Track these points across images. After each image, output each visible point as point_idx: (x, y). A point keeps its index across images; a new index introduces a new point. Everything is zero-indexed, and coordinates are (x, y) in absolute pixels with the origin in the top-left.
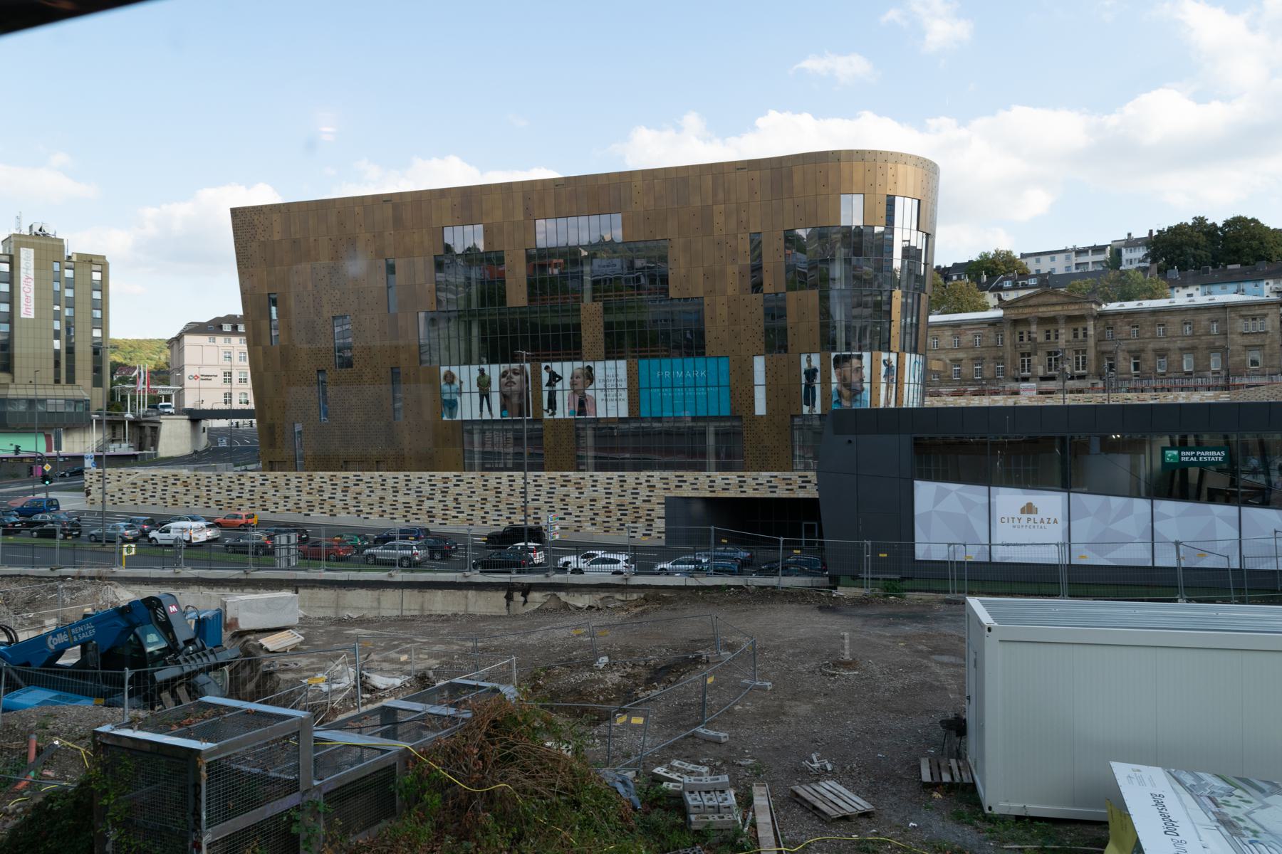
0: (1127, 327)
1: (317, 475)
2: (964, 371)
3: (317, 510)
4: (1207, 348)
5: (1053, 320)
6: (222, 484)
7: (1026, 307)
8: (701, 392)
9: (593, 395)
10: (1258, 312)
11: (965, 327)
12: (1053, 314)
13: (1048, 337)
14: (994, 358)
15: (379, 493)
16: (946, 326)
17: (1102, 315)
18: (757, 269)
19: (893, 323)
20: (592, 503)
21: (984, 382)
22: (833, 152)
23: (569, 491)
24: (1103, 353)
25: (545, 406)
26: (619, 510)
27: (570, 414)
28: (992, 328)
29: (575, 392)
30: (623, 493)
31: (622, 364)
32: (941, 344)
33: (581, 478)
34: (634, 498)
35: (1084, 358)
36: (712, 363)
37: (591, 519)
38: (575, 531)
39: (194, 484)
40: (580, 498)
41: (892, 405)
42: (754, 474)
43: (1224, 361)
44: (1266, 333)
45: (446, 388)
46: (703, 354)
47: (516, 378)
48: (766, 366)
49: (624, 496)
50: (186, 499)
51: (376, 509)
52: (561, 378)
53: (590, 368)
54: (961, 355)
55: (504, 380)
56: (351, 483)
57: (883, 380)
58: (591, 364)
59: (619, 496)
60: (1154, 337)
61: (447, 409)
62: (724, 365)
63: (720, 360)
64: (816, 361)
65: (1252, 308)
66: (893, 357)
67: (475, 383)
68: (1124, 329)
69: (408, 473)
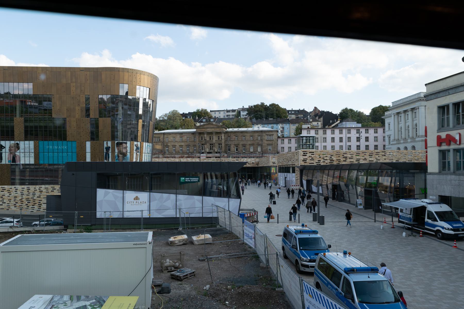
0: (234, 137)
2: (184, 149)
4: (257, 144)
5: (211, 133)
7: (203, 128)
8: (65, 154)
9: (19, 155)
10: (271, 134)
11: (183, 134)
12: (211, 131)
13: (210, 139)
14: (193, 145)
16: (177, 133)
17: (227, 132)
18: (88, 110)
19: (139, 131)
20: (15, 198)
21: (190, 154)
22: (117, 68)
23: (4, 193)
24: (227, 145)
26: (27, 201)
27: (8, 162)
28: (193, 135)
29: (11, 153)
30: (29, 194)
31: (32, 143)
32: (176, 140)
33: (10, 188)
34: (33, 196)
35: (221, 146)
36: (70, 144)
37: (14, 205)
38: (7, 210)
40: (9, 196)
41: (138, 161)
43: (262, 149)
44: (273, 140)
46: (65, 139)
48: (91, 145)
49: (29, 195)
52: (4, 147)
54: (183, 144)
57: (135, 152)
58: (18, 142)
59: (27, 195)
60: (242, 140)
62: (74, 144)
63: (73, 142)
64: (110, 144)
65: (269, 132)
66: (139, 143)
68: (233, 137)
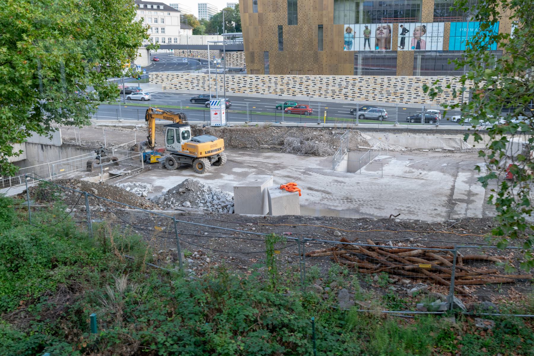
1: (286, 77)
6: (235, 80)
15: (319, 85)
25: (399, 44)
27: (412, 48)
29: (415, 38)
31: (442, 25)
39: (219, 80)
45: (346, 35)
47: (385, 31)
52: (408, 31)
53: (424, 27)
55: (378, 32)
56: (304, 80)
67: (362, 33)
69: (334, 76)
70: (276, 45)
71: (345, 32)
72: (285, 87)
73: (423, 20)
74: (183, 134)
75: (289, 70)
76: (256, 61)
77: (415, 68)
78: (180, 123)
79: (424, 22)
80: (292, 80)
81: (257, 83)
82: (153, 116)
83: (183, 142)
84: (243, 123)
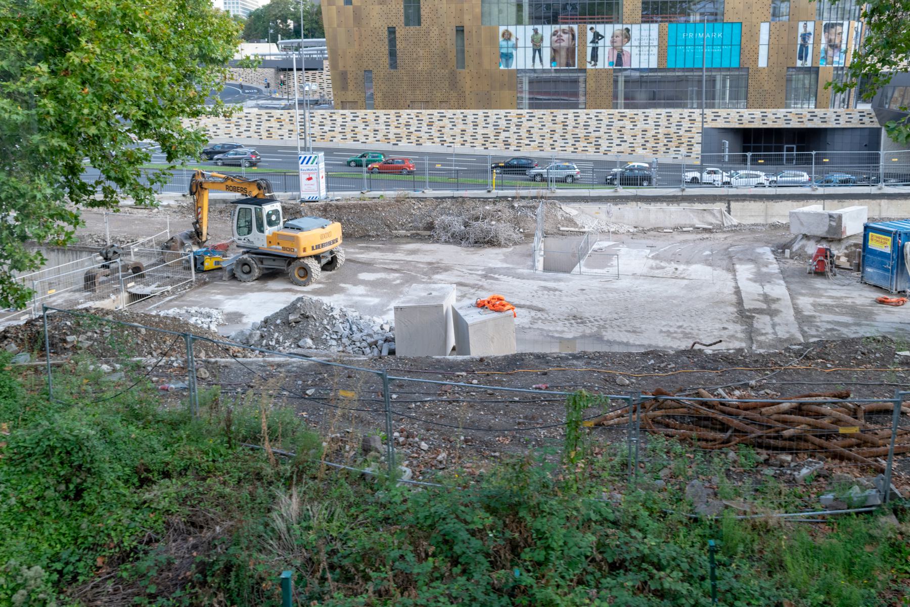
1: (404, 113)
3: (404, 140)
6: (315, 120)
8: (717, 50)
15: (461, 126)
25: (589, 58)
27: (609, 65)
29: (614, 48)
31: (655, 27)
39: (287, 120)
42: (774, 111)
45: (503, 43)
47: (565, 37)
50: (280, 132)
51: (458, 139)
52: (603, 37)
55: (555, 38)
56: (435, 119)
61: (504, 60)
67: (529, 40)
70: (385, 60)
71: (501, 39)
72: (403, 131)
73: (626, 20)
74: (269, 215)
75: (408, 102)
76: (351, 87)
77: (616, 97)
78: (261, 197)
79: (626, 23)
80: (416, 118)
81: (354, 124)
82: (205, 186)
83: (269, 230)
84: (357, 194)
